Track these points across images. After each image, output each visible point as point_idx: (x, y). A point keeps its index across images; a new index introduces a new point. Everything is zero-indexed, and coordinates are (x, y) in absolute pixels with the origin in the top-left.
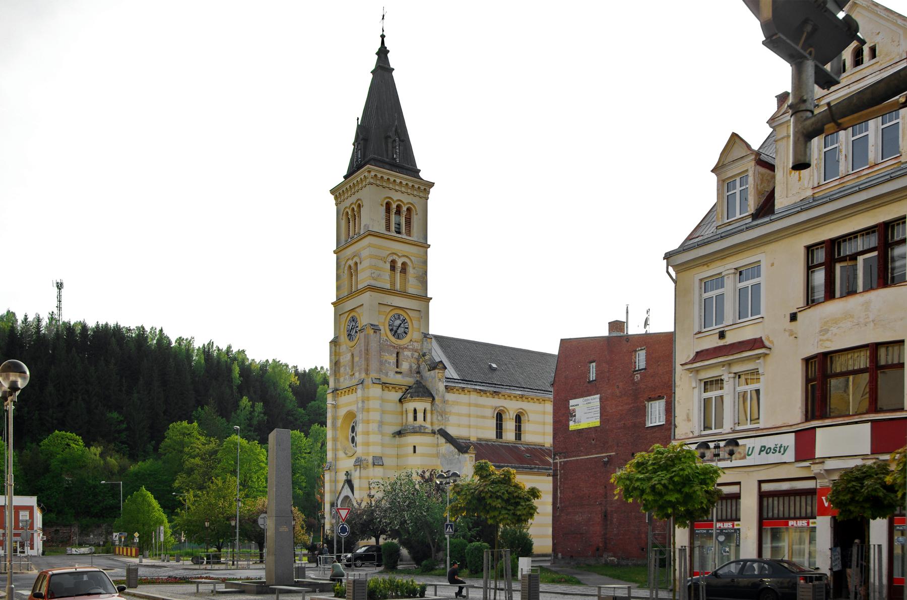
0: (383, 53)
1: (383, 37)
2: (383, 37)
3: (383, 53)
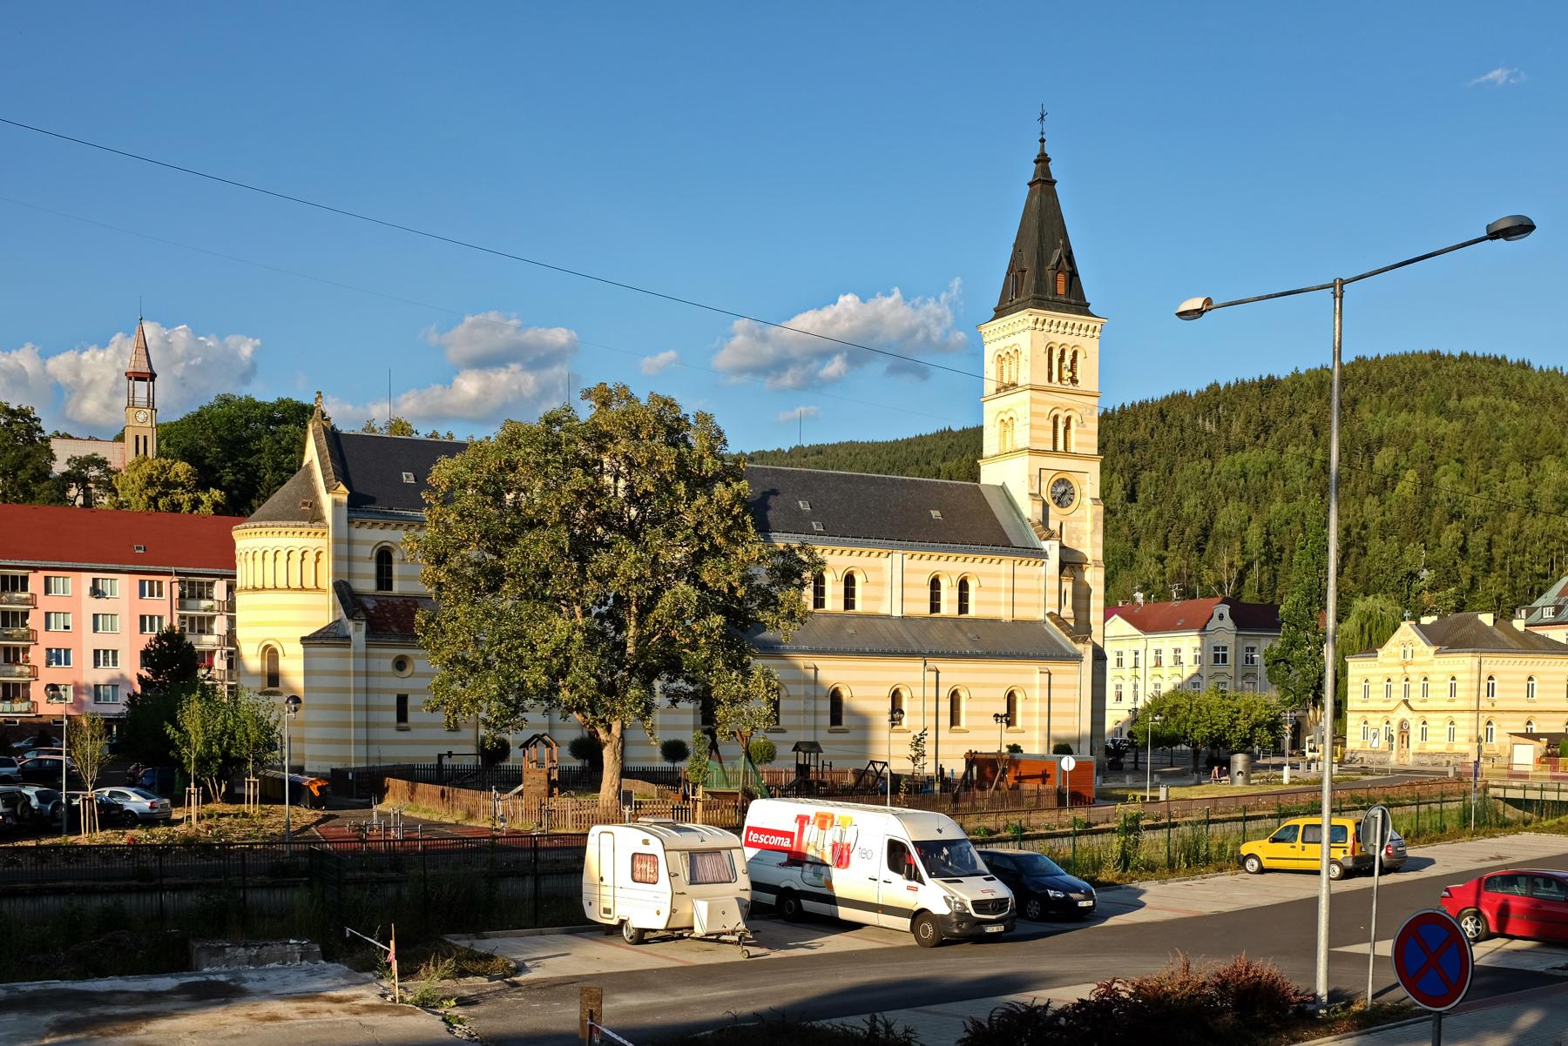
0: (1043, 160)
1: (1043, 141)
2: (1043, 141)
3: (1043, 160)
